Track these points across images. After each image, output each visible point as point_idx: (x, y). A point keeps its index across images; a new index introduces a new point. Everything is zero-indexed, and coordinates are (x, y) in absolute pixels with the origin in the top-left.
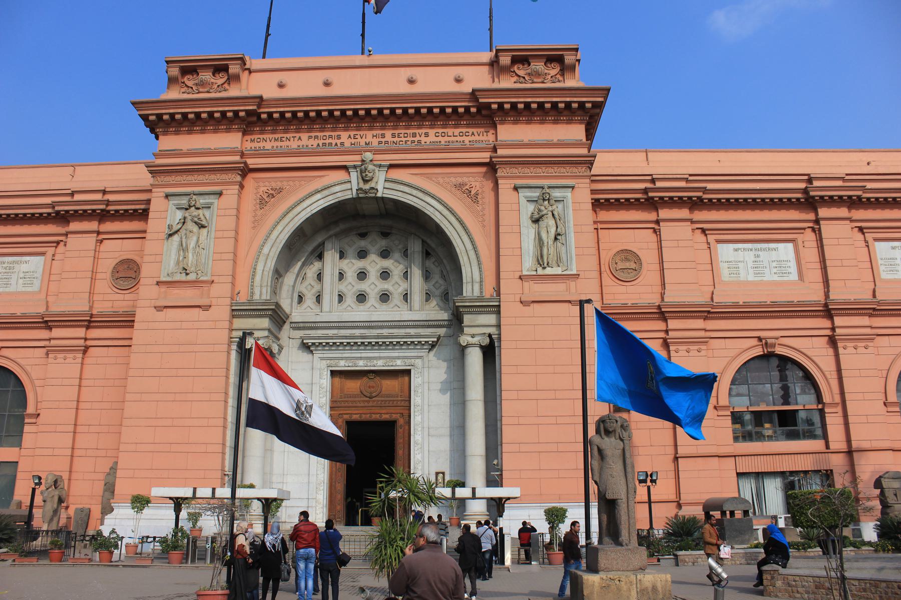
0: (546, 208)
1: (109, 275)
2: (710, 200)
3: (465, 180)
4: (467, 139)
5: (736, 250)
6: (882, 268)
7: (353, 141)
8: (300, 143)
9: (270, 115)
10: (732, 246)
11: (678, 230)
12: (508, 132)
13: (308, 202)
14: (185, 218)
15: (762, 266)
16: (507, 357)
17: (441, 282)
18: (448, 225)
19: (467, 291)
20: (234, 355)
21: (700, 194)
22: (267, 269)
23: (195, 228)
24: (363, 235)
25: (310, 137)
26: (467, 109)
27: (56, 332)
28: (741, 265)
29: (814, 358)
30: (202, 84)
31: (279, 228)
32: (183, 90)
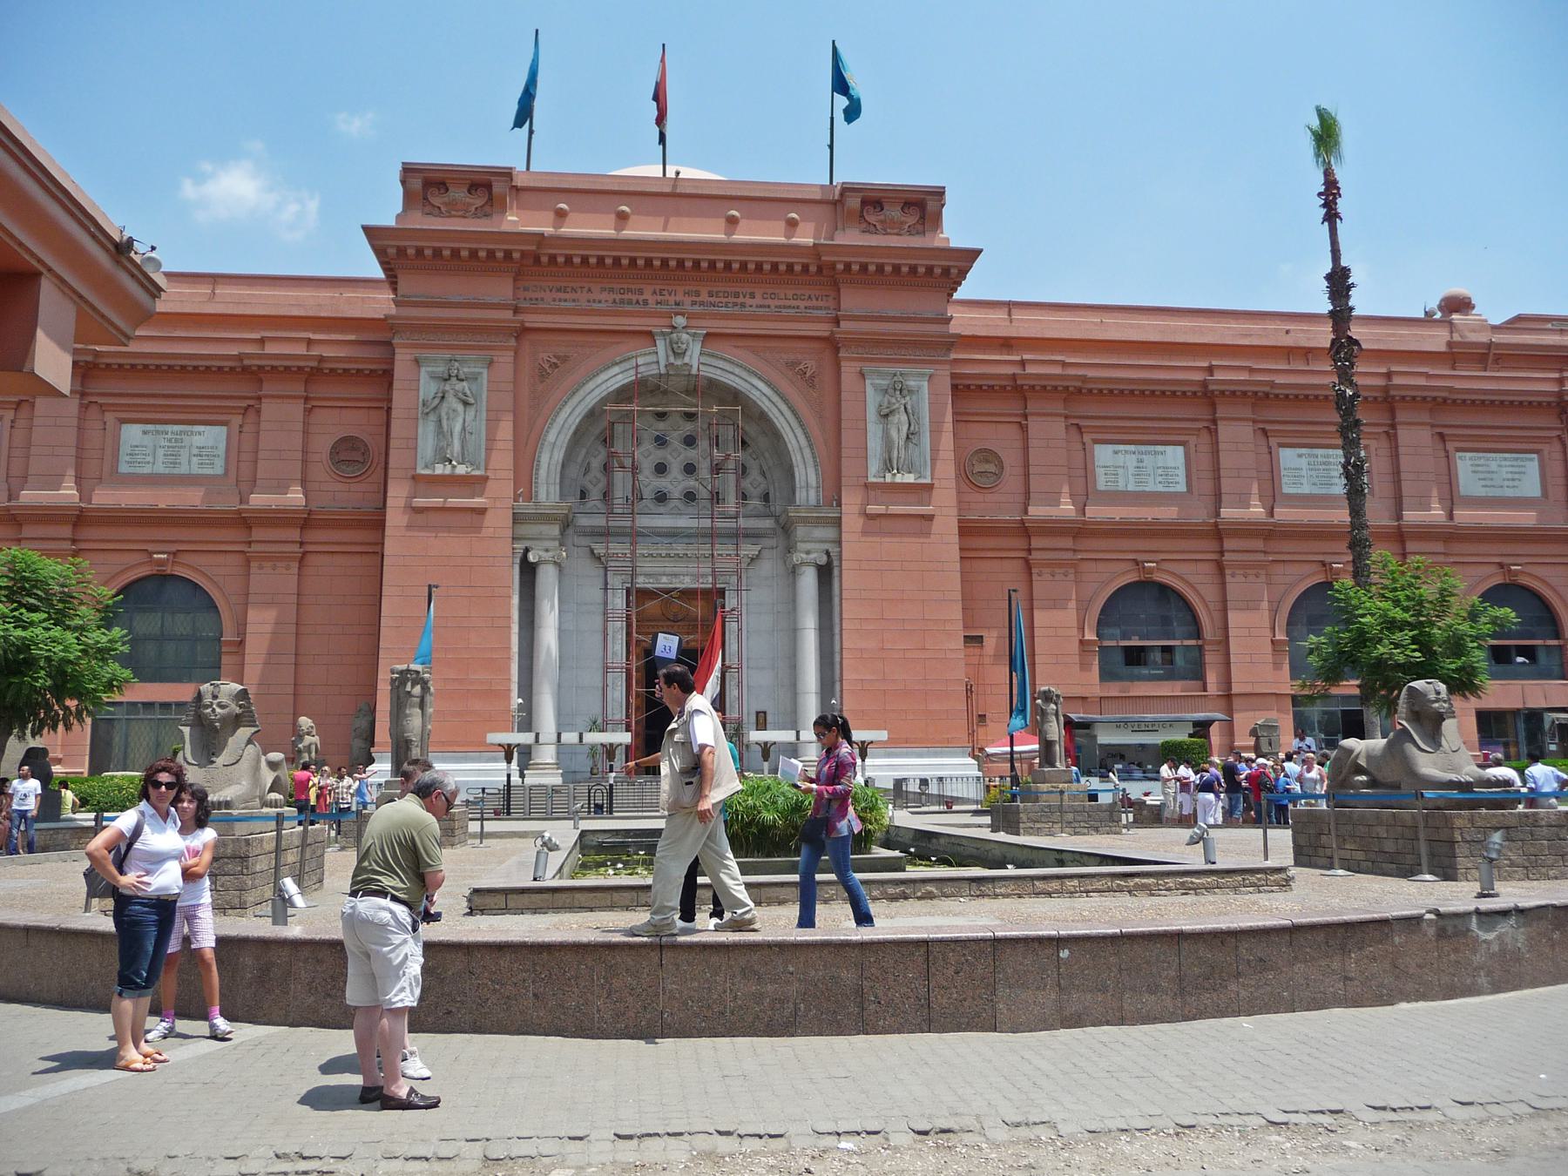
0: (898, 402)
1: (325, 456)
2: (1090, 391)
3: (800, 357)
4: (802, 304)
5: (1116, 453)
6: (1284, 480)
7: (660, 298)
8: (591, 296)
9: (553, 258)
10: (1111, 448)
11: (1048, 430)
12: (854, 301)
13: (603, 377)
14: (444, 393)
15: (1143, 473)
16: (848, 580)
17: (760, 479)
18: (778, 414)
19: (800, 496)
20: (517, 568)
21: (1079, 384)
22: (553, 462)
23: (460, 408)
24: (661, 416)
25: (603, 290)
26: (805, 268)
27: (257, 534)
28: (1120, 471)
29: (1199, 587)
30: (452, 205)
31: (568, 409)
32: (428, 209)
